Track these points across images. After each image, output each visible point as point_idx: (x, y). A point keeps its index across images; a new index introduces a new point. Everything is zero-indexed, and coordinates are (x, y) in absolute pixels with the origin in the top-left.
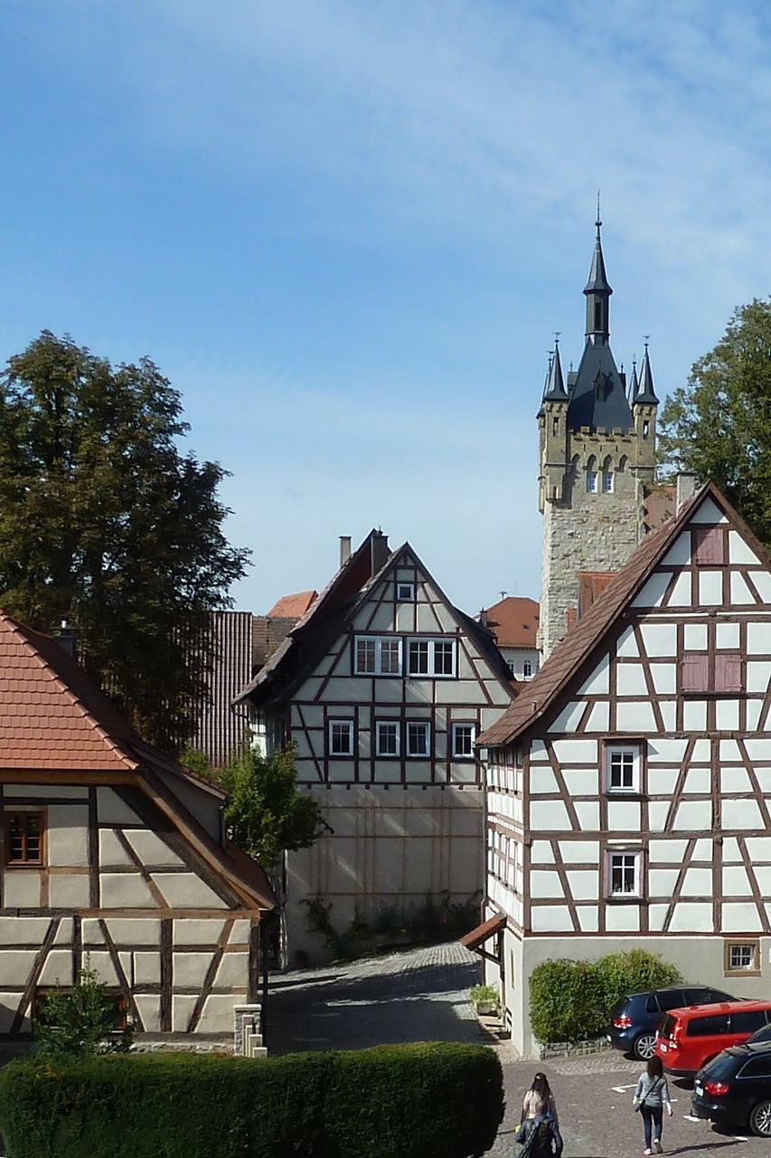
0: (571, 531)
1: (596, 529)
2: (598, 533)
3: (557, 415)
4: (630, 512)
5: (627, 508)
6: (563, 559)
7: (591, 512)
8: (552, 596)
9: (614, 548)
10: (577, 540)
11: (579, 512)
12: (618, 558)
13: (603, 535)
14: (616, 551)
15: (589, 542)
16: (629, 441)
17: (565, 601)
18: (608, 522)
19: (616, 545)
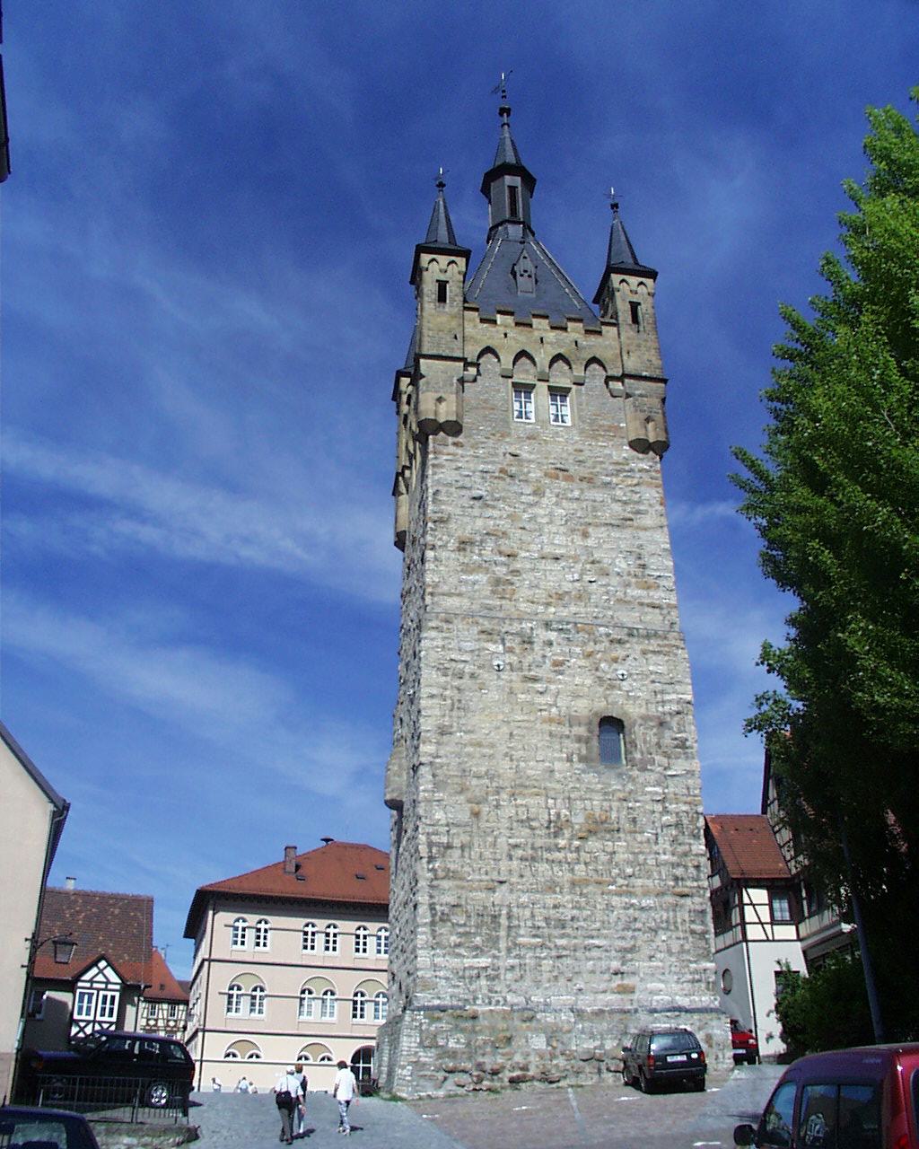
0: (476, 493)
1: (538, 492)
2: (545, 500)
3: (442, 277)
4: (618, 463)
5: (610, 455)
6: (459, 550)
7: (525, 455)
8: (433, 634)
9: (585, 535)
10: (496, 513)
11: (497, 455)
12: (597, 556)
13: (557, 504)
14: (590, 542)
15: (526, 516)
16: (600, 333)
17: (468, 645)
18: (570, 479)
19: (590, 530)
